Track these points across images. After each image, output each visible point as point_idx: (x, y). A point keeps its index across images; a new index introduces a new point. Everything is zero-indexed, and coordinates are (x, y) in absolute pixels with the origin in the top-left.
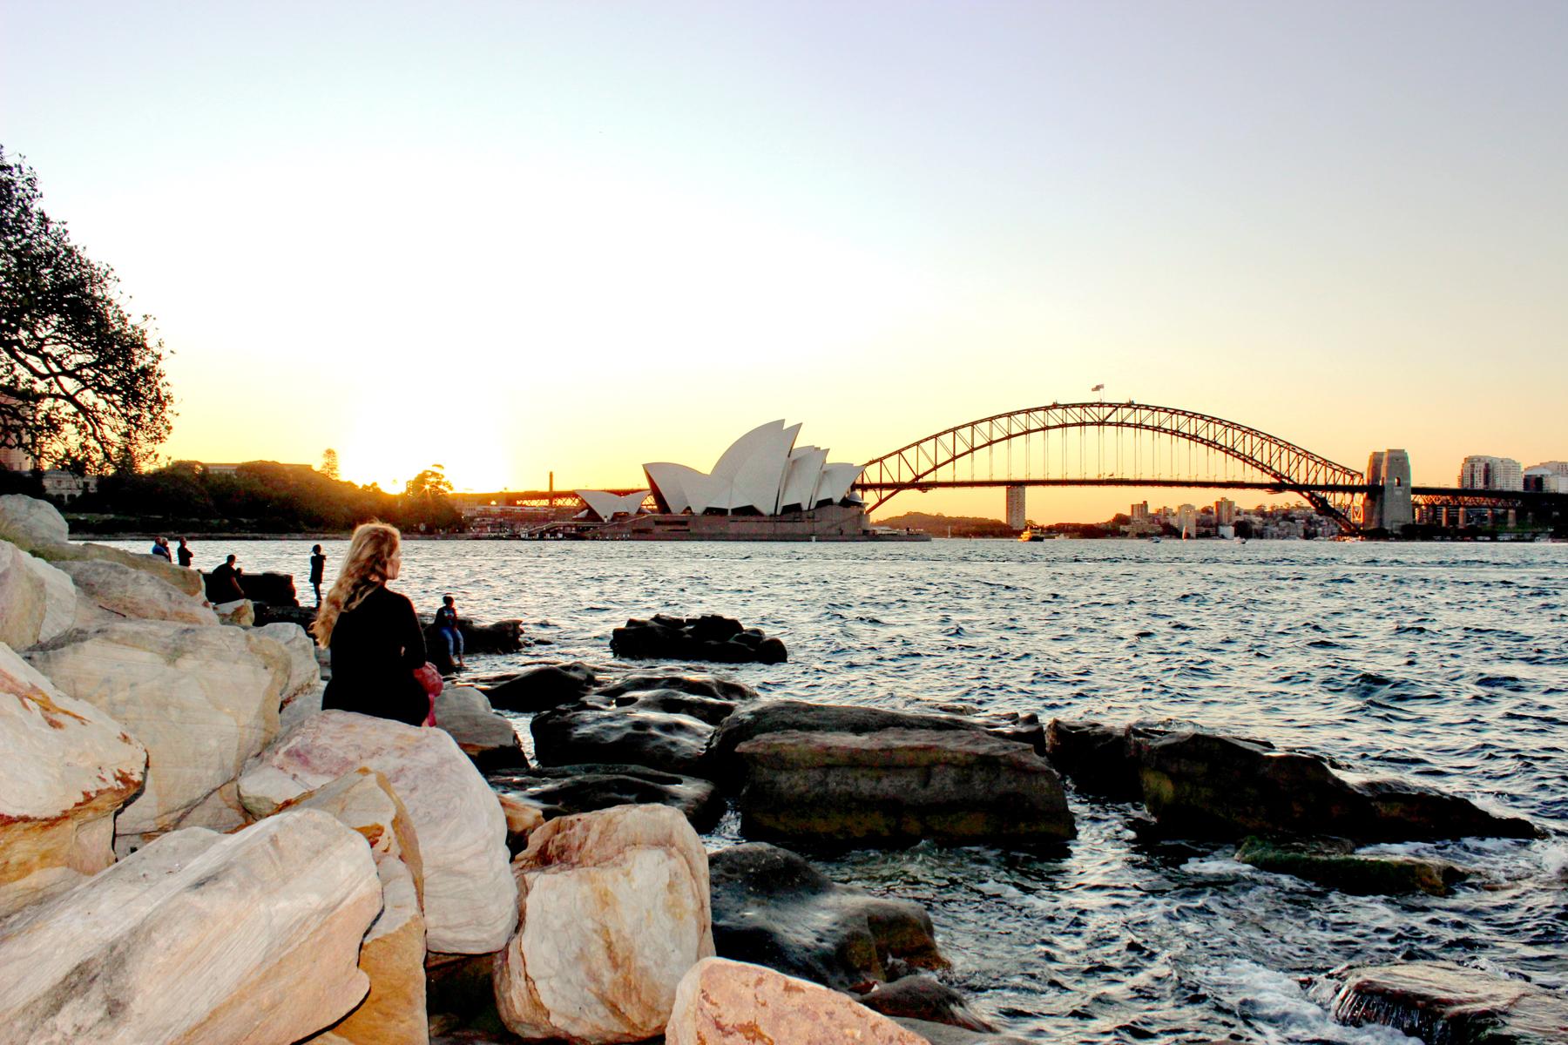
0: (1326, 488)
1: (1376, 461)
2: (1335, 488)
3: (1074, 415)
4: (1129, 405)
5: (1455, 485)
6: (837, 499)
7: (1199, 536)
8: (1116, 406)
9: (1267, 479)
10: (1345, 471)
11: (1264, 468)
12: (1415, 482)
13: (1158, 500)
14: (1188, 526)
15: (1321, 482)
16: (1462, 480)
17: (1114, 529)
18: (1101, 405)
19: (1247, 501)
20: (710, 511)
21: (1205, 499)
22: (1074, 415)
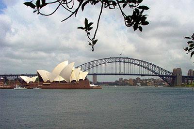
0: (165, 76)
1: (174, 70)
2: (167, 76)
3: (114, 60)
4: (127, 58)
5: (186, 75)
6: (84, 79)
7: (134, 85)
8: (123, 58)
9: (154, 74)
10: (169, 72)
11: (152, 71)
12: (183, 75)
13: (124, 77)
14: (132, 83)
15: (164, 75)
16: (188, 75)
17: (116, 83)
18: (120, 58)
19: (142, 78)
20: (54, 81)
21: (134, 77)
22: (114, 60)
